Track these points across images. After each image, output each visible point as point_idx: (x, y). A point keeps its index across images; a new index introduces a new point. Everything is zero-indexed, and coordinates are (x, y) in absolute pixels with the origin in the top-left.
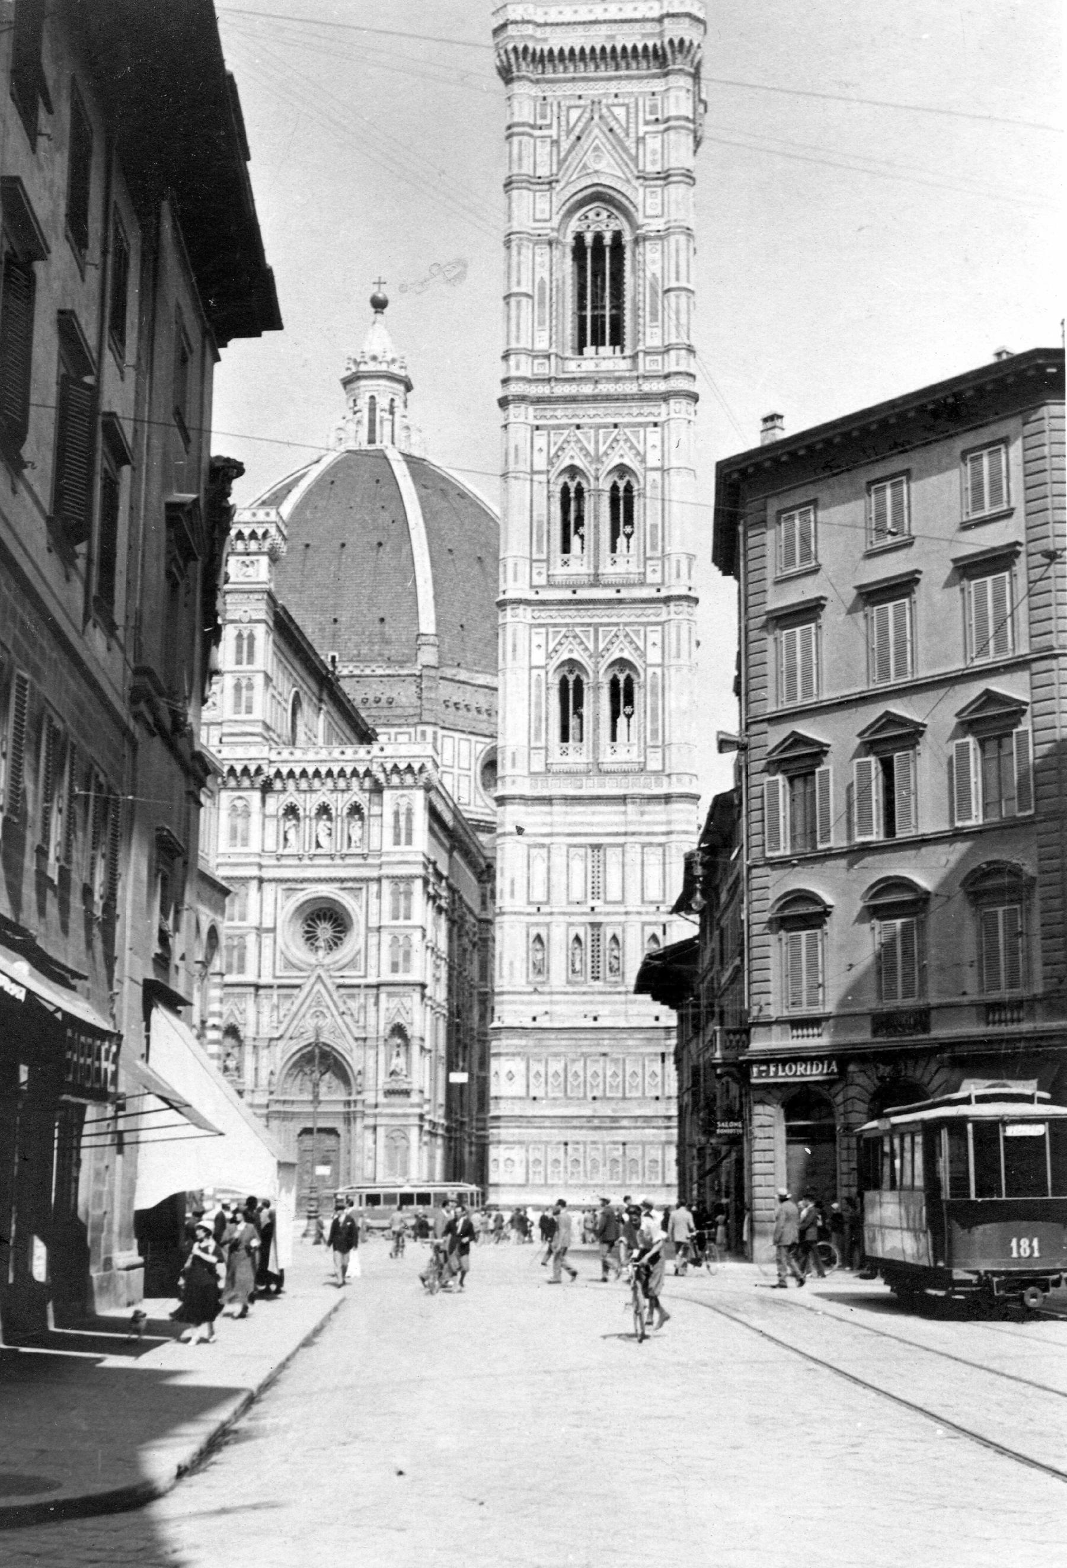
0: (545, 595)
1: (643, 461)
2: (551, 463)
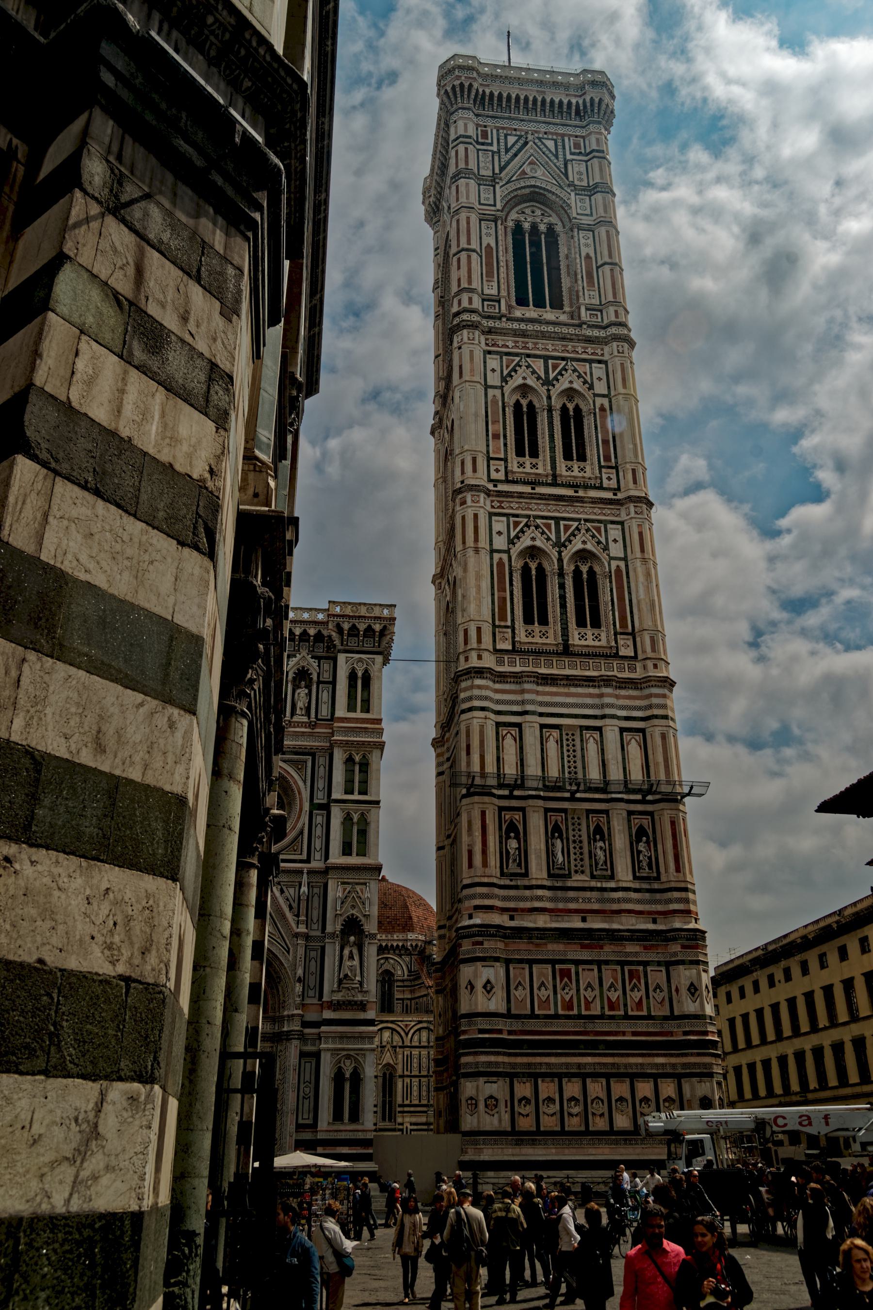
0: (501, 487)
1: (591, 387)
2: (504, 380)
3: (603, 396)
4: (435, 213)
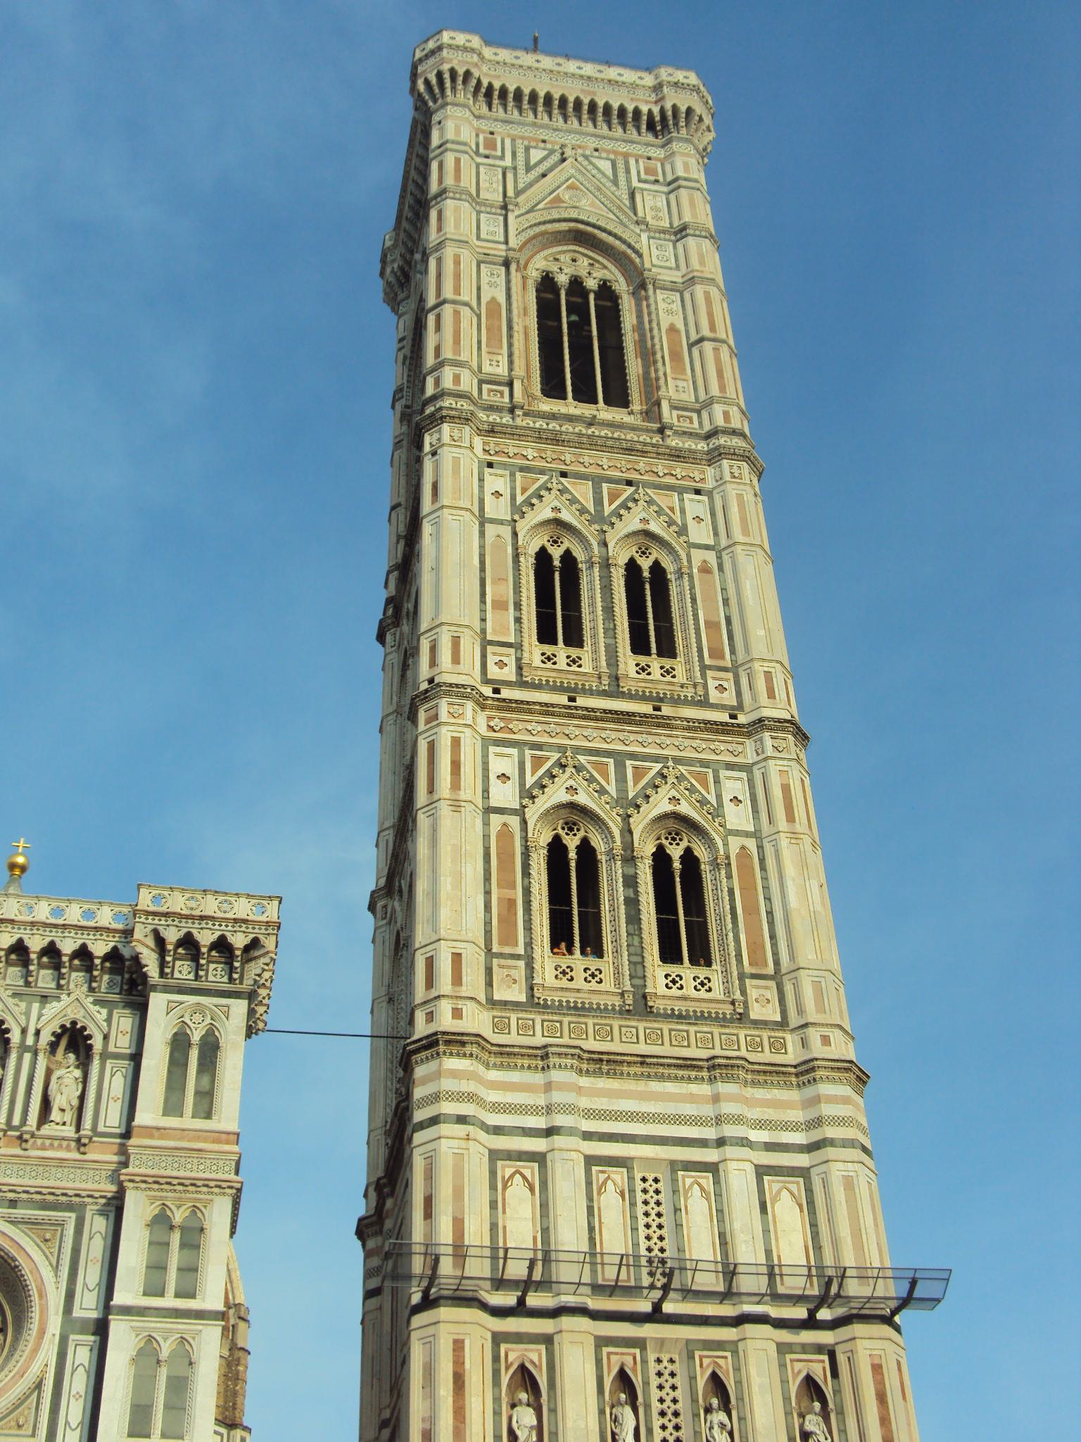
1: (683, 531)
2: (518, 511)
3: (707, 547)
4: (402, 285)
